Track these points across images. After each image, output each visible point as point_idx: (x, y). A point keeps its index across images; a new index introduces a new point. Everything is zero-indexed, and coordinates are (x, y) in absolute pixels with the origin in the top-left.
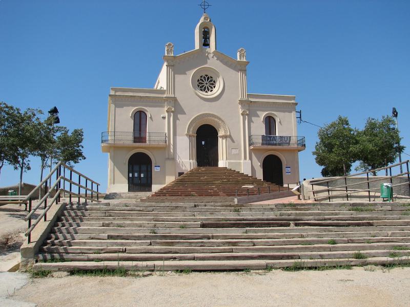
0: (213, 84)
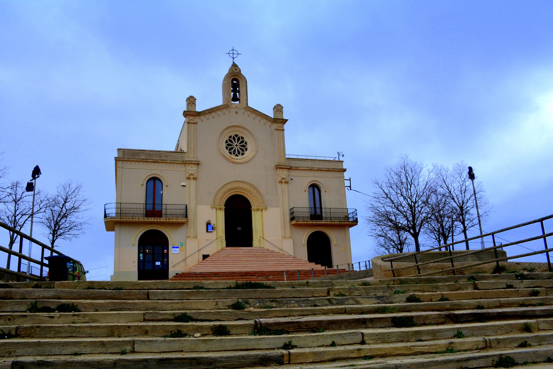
0: (244, 148)
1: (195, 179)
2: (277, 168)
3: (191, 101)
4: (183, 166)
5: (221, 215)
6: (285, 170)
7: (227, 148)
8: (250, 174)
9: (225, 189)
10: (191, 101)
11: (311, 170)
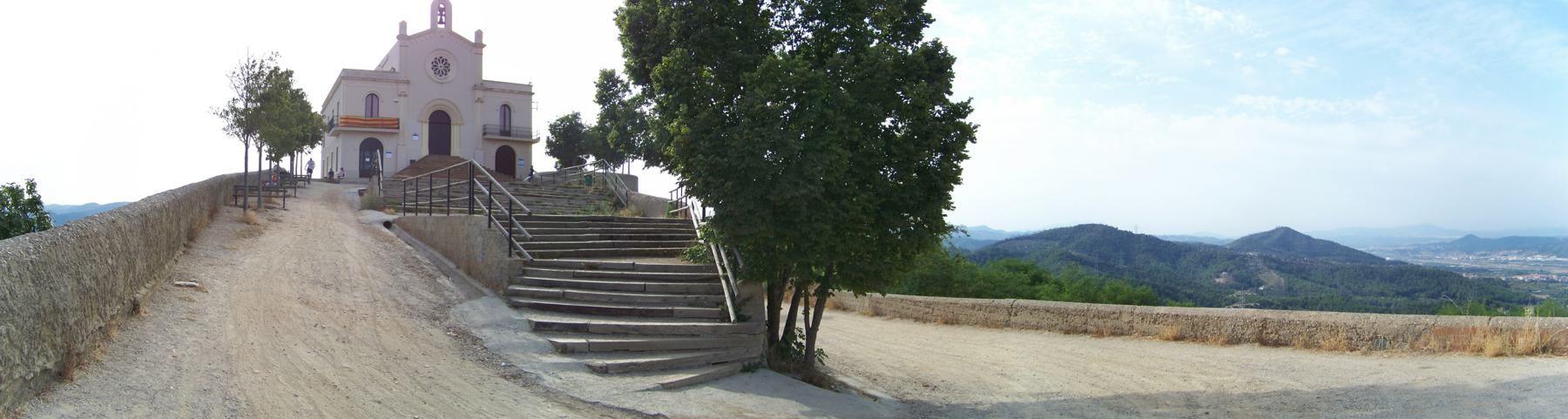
3: (403, 26)
5: (426, 128)
8: (449, 94)
10: (403, 26)
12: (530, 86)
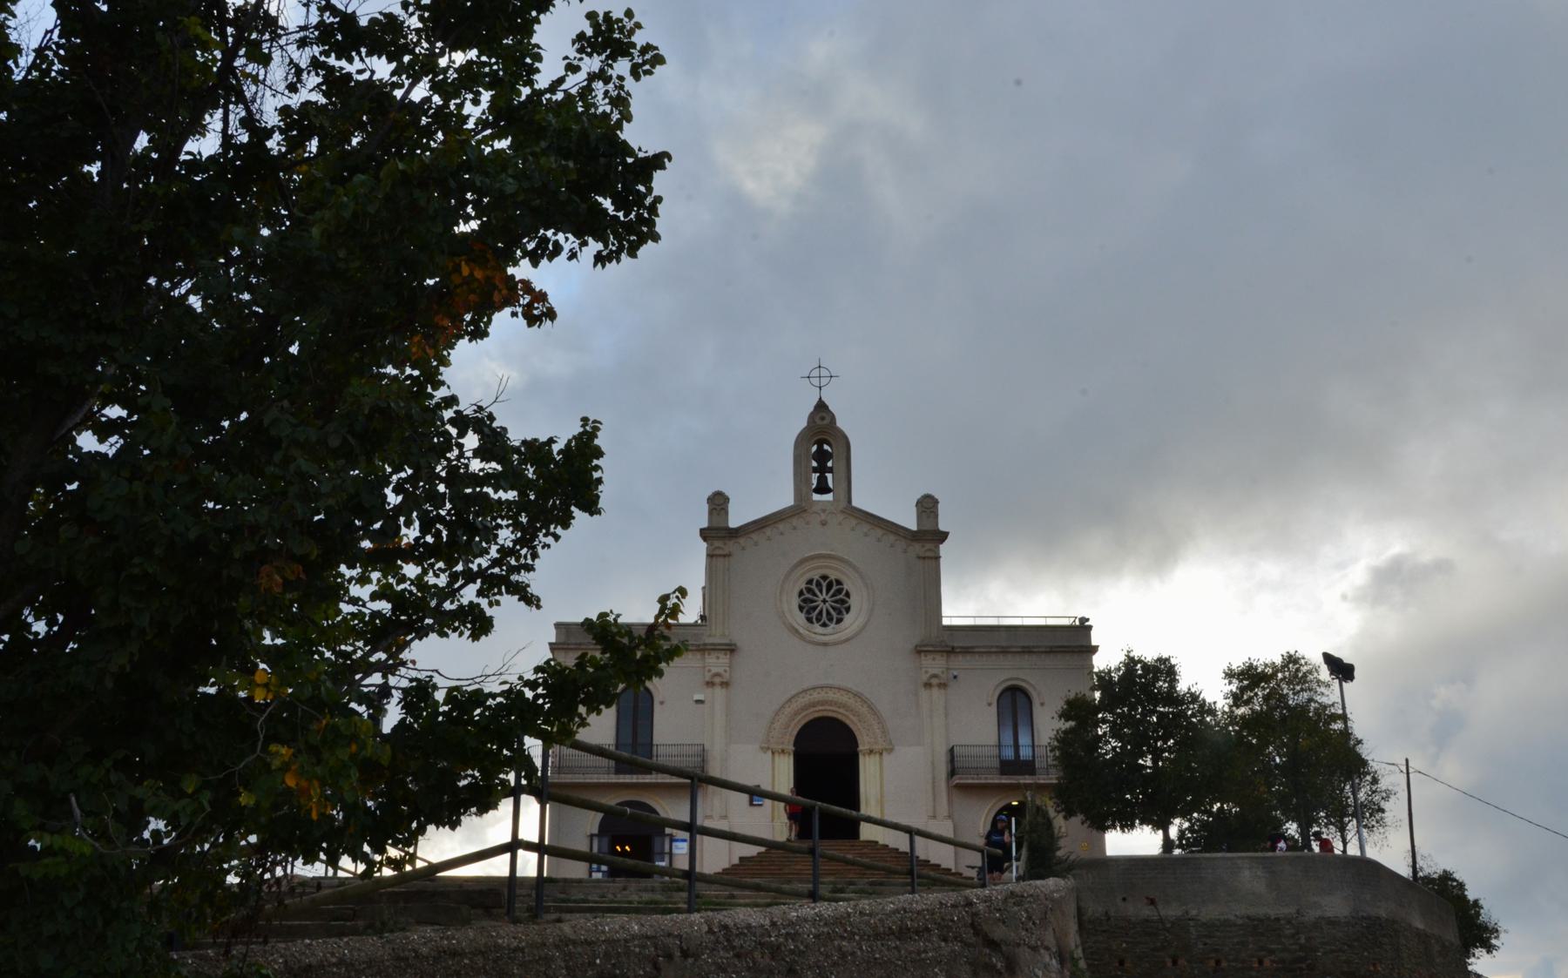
0: (842, 606)
1: (725, 684)
2: (919, 652)
3: (718, 503)
4: (698, 655)
6: (938, 656)
7: (801, 608)
8: (852, 667)
9: (795, 705)
10: (718, 503)
11: (1004, 651)
12: (1083, 628)
